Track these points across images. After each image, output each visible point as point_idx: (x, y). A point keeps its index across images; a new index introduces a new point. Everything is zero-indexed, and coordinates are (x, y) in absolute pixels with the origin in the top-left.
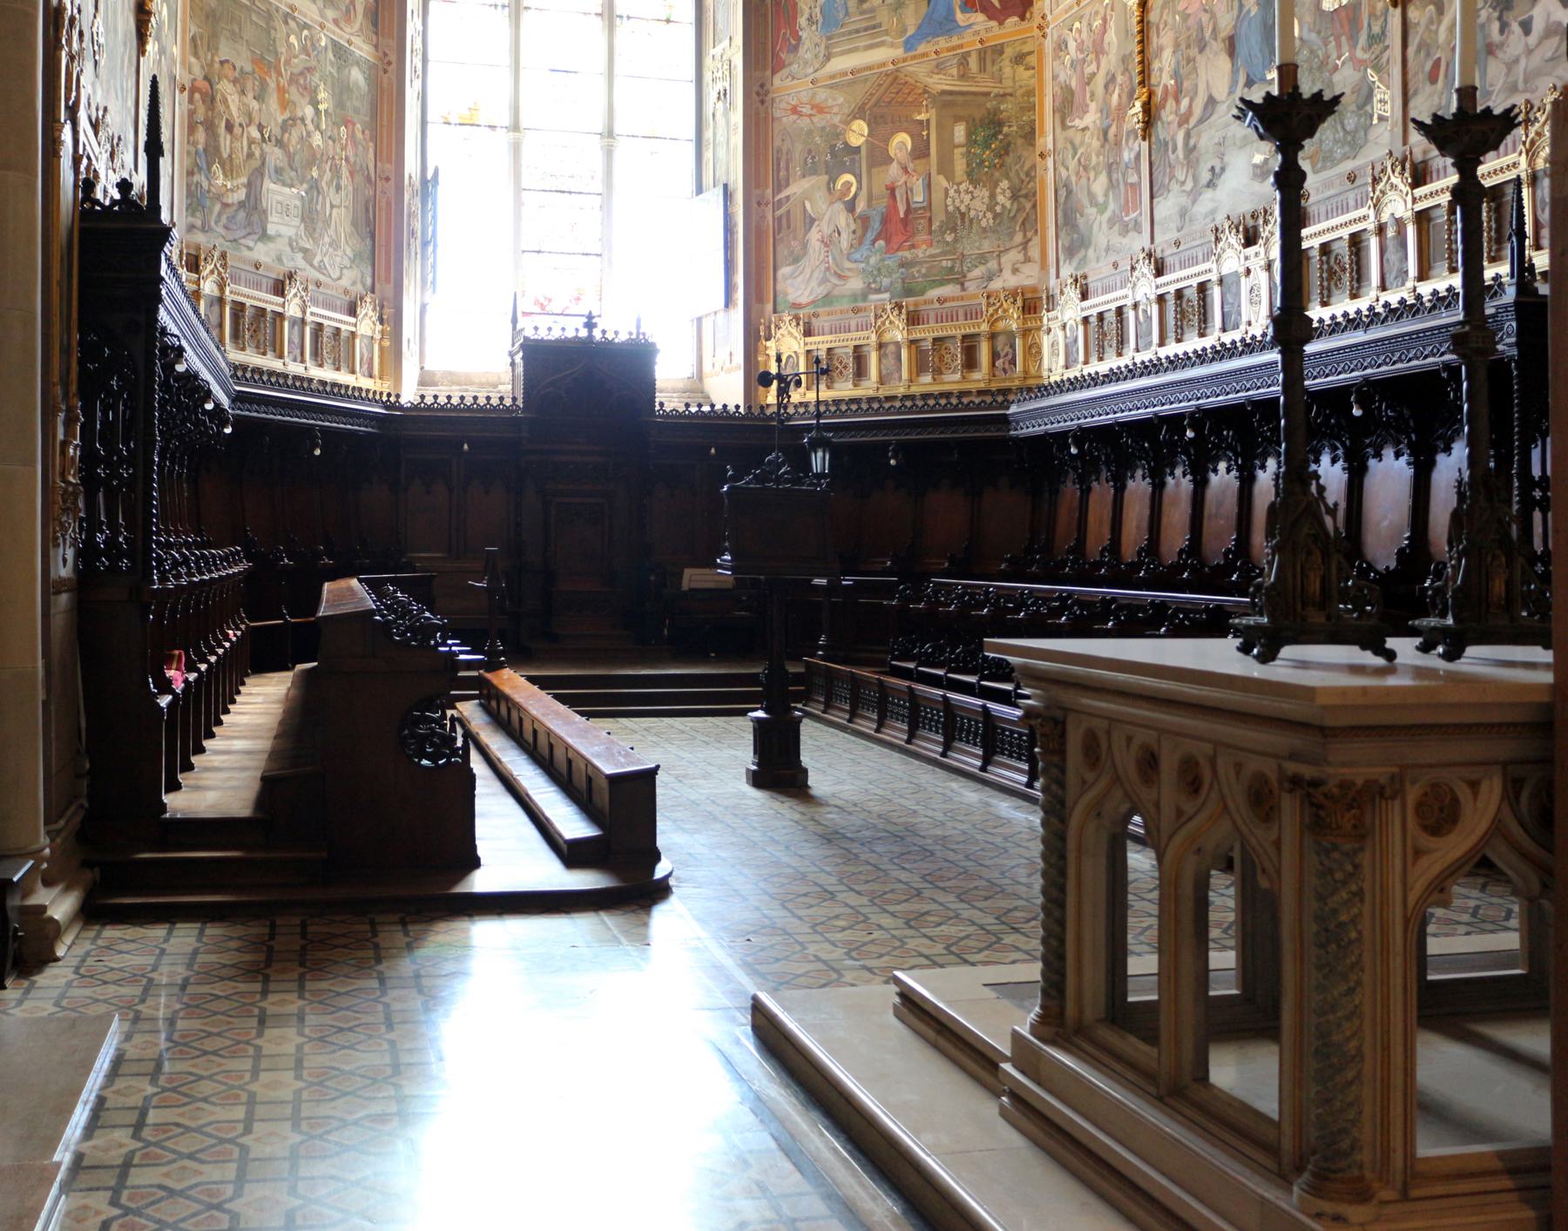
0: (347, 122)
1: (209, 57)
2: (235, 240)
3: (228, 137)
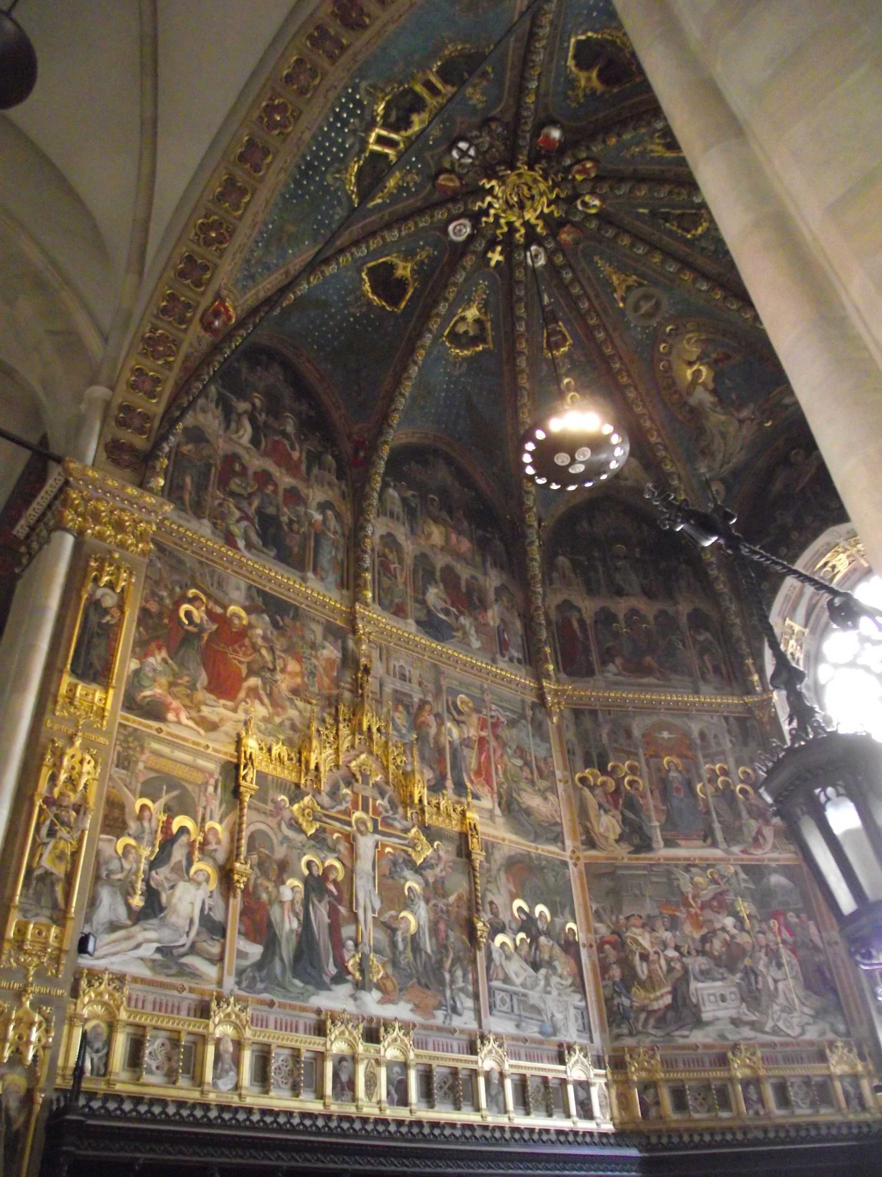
0: (775, 915)
1: (614, 918)
2: (668, 1034)
3: (645, 965)
